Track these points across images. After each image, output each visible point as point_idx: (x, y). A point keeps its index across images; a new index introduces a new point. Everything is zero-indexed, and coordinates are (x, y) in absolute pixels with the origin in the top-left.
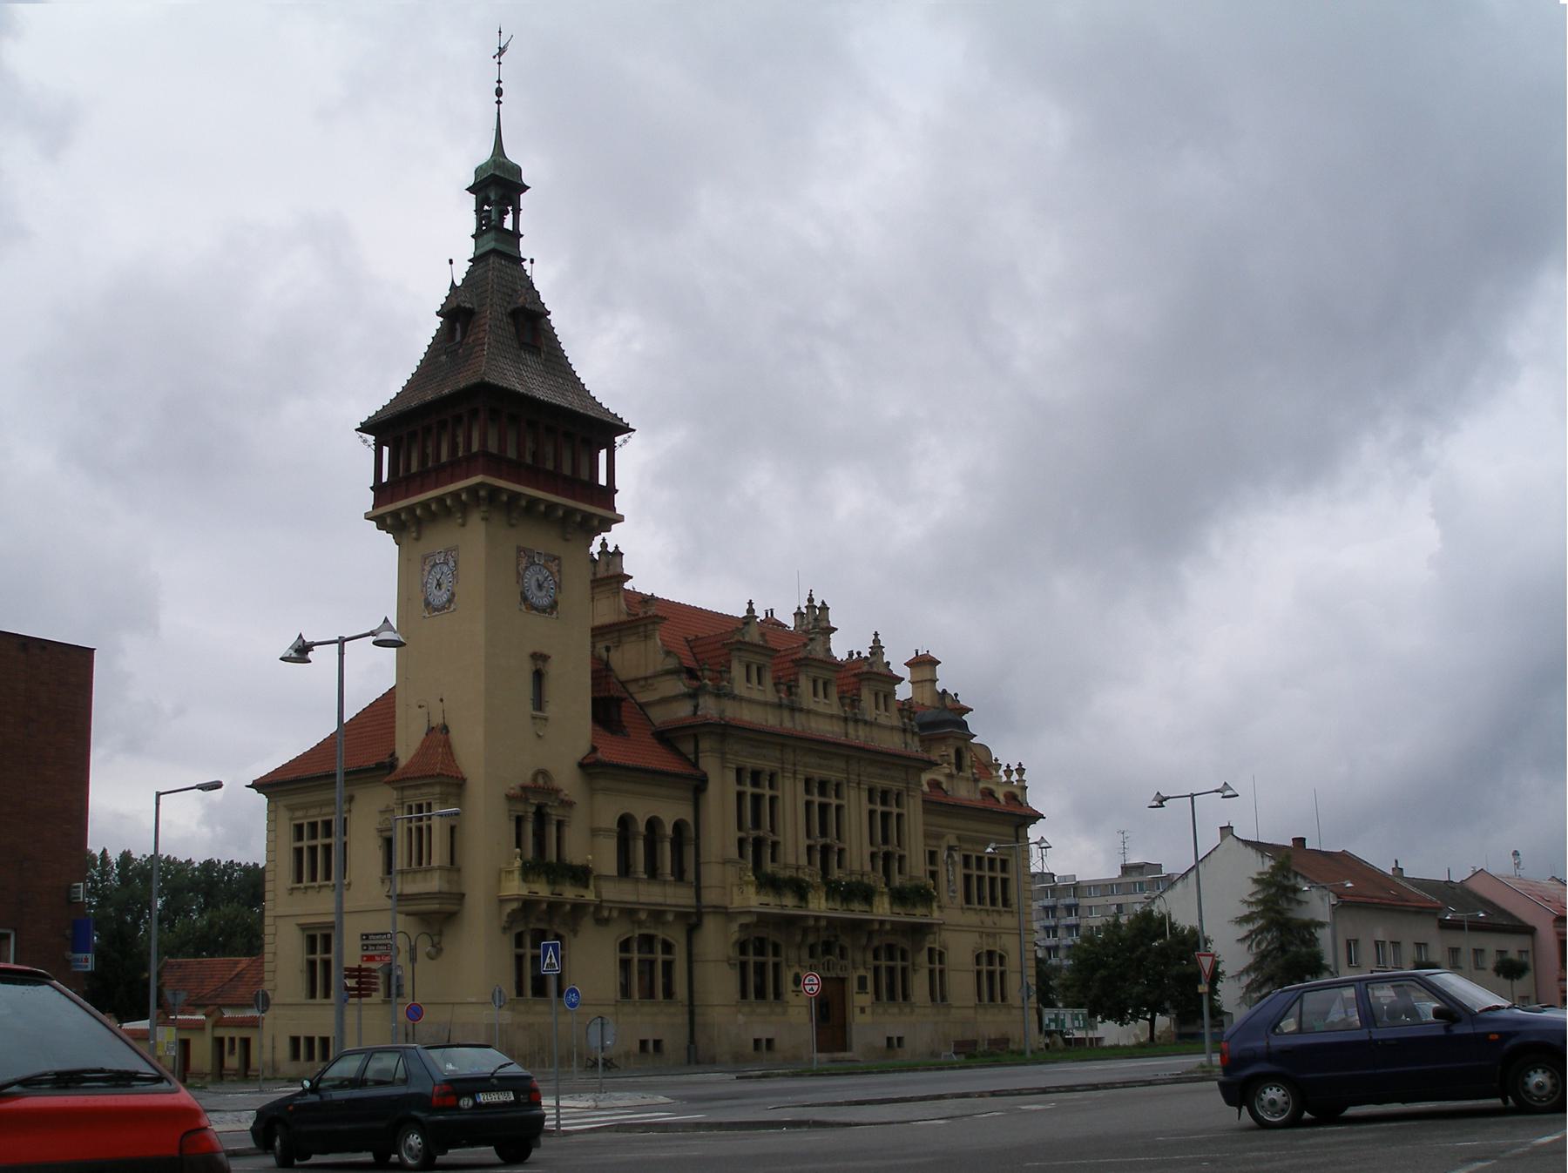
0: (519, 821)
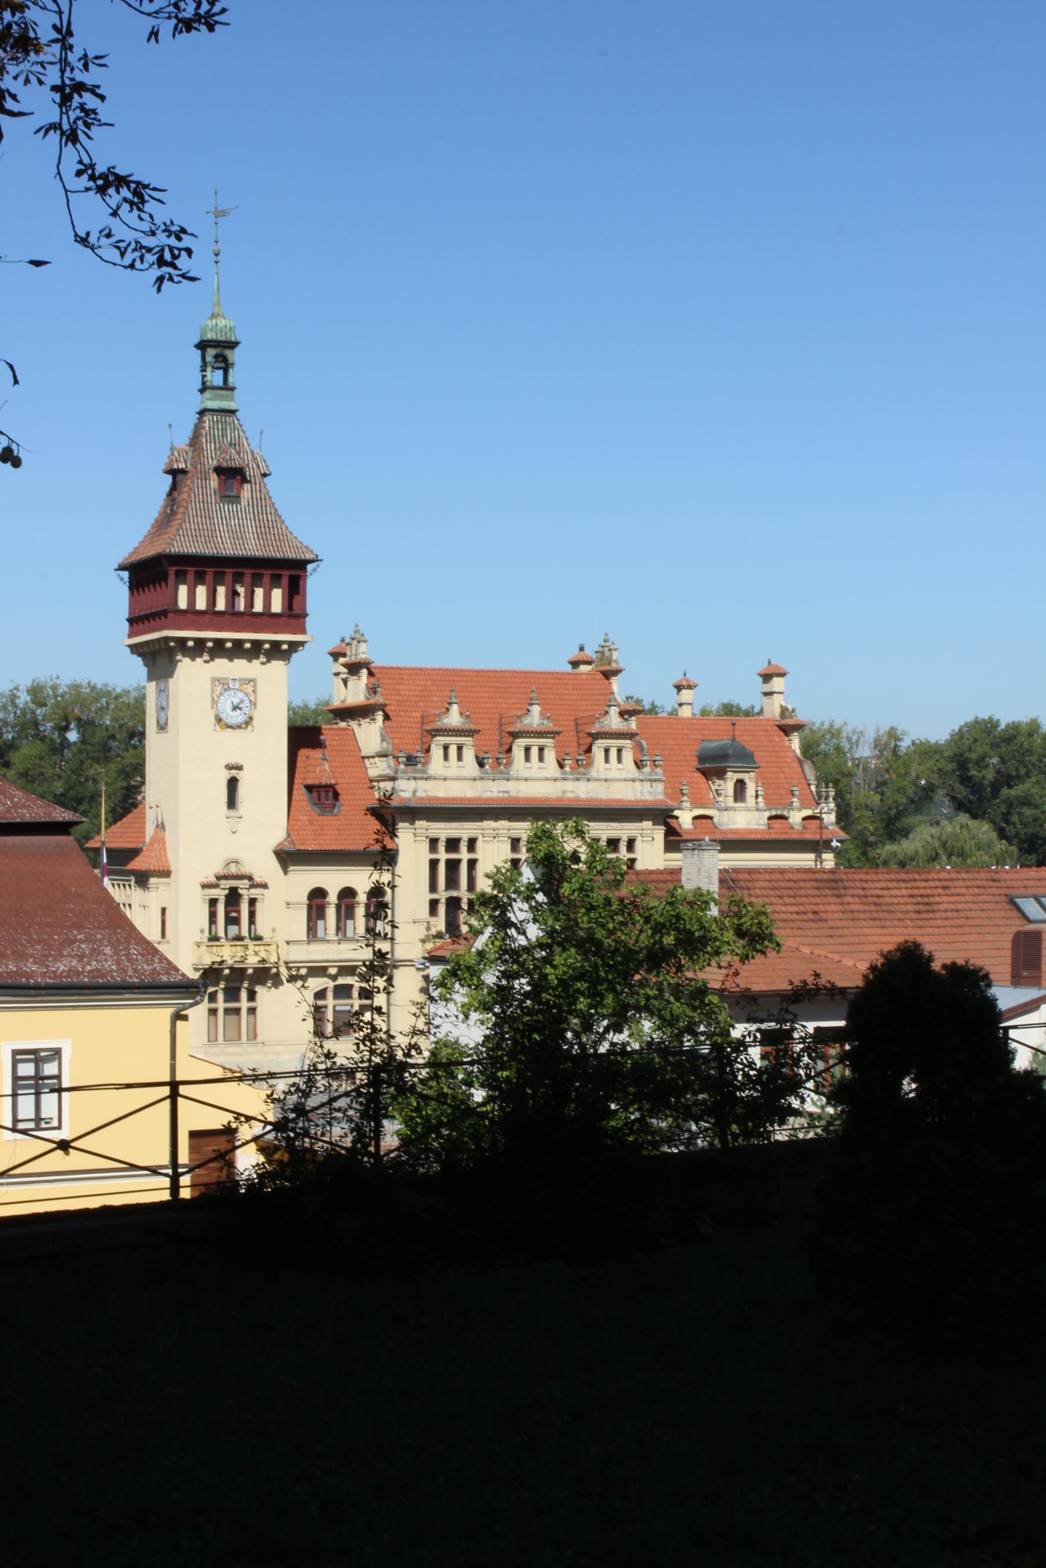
0: (213, 902)
